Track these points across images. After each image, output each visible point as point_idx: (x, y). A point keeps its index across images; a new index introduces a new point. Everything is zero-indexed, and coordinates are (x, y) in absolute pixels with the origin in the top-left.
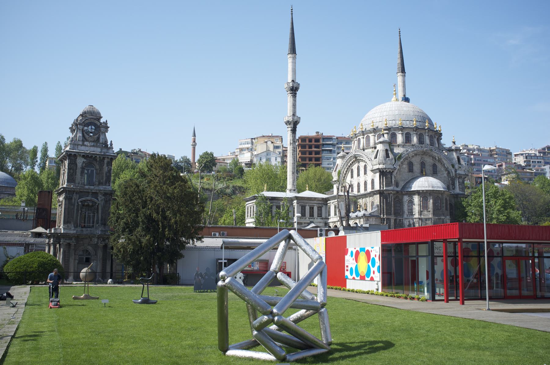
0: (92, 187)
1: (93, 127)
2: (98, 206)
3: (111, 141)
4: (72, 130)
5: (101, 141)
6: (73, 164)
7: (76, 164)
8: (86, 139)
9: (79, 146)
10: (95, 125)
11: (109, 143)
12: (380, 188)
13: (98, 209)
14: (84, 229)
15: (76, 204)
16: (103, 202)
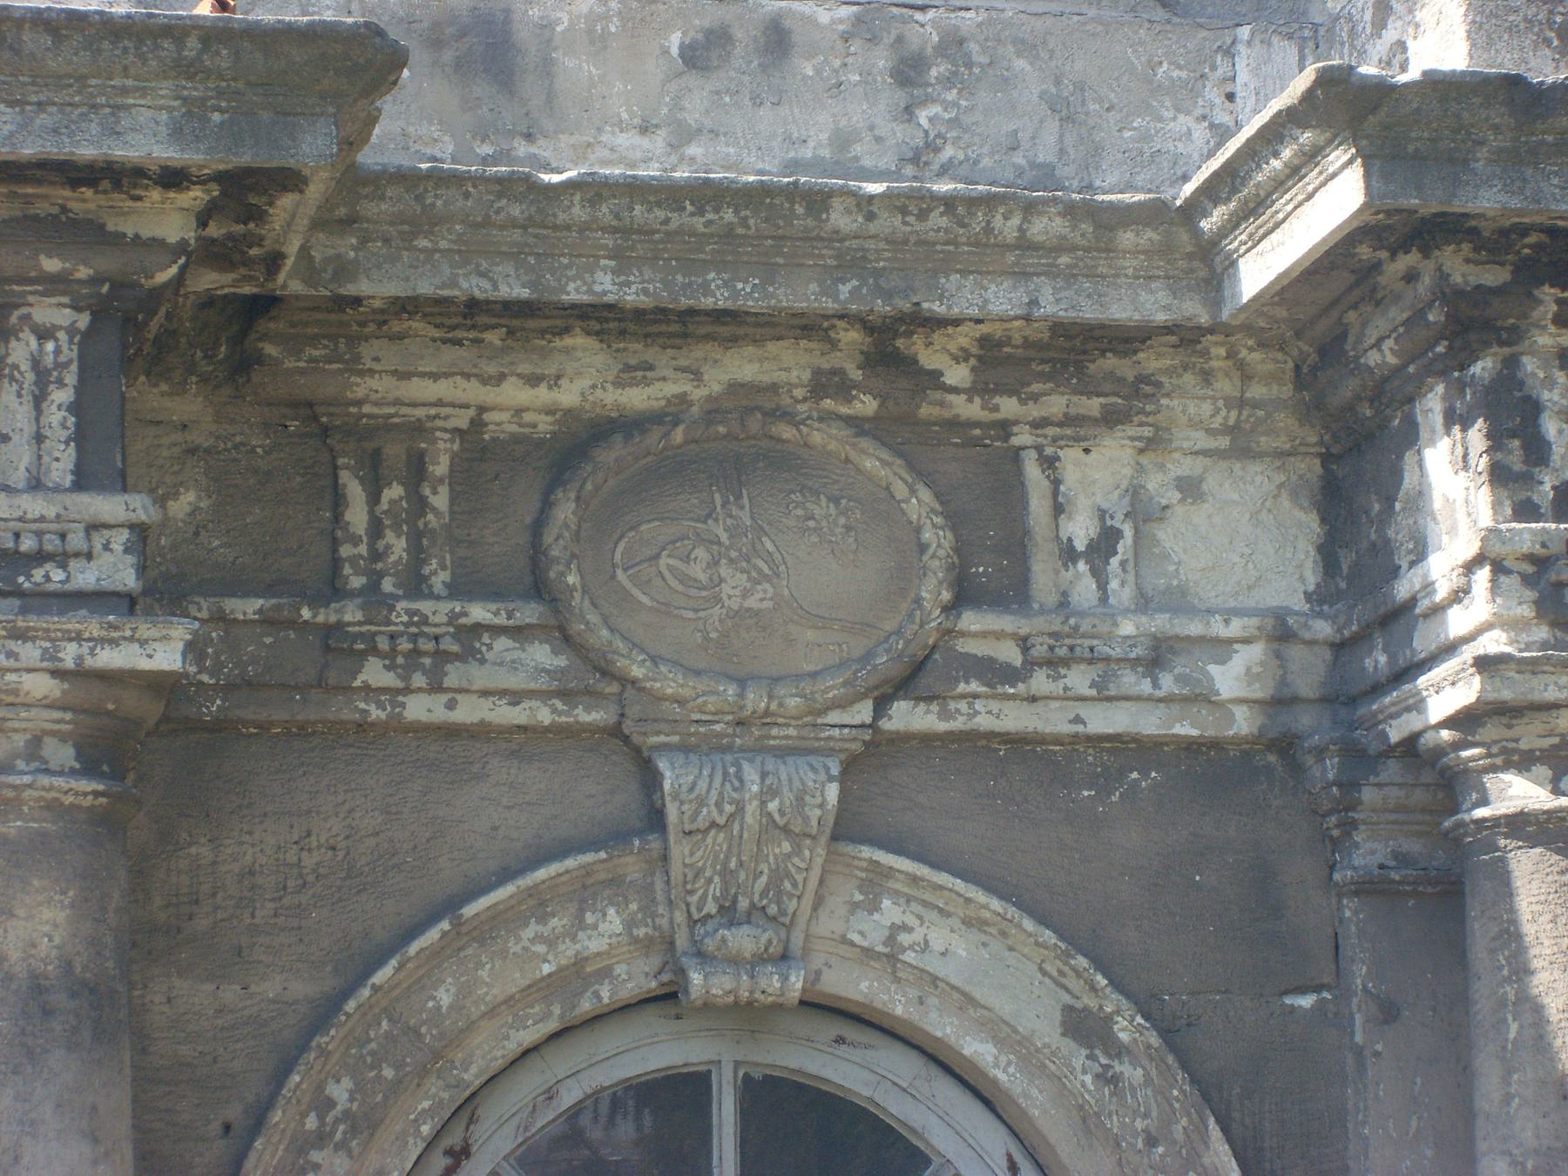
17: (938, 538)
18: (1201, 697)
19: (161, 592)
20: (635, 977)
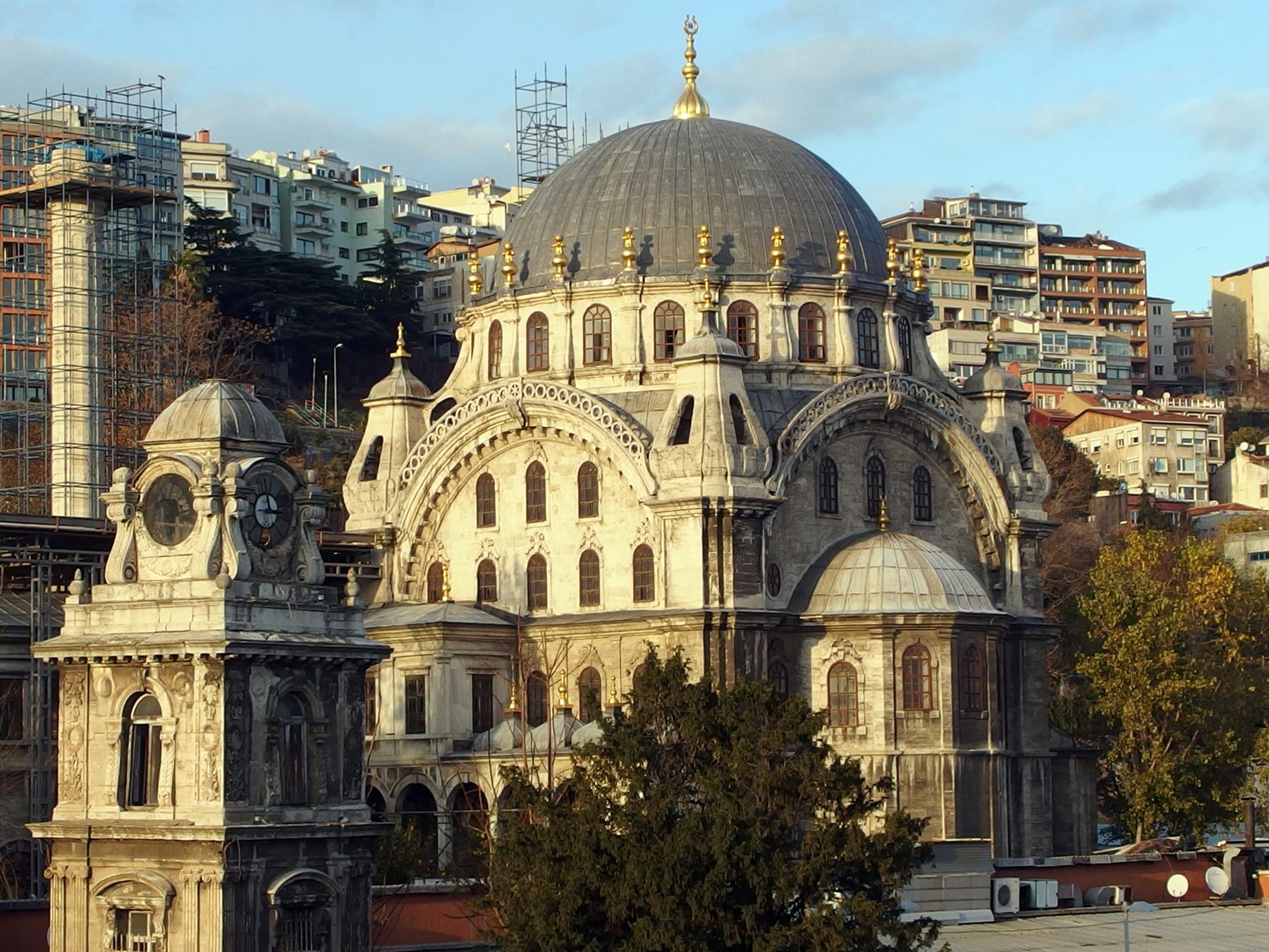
0: (307, 814)
9: (255, 611)
12: (706, 600)
16: (347, 880)
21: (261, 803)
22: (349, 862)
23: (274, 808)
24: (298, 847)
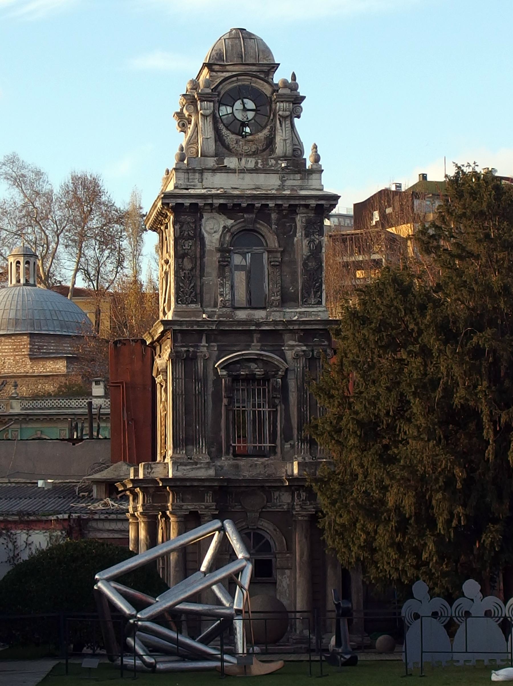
0: (260, 315)
1: (250, 104)
2: (284, 378)
3: (315, 147)
4: (183, 122)
5: (280, 148)
6: (190, 238)
7: (202, 239)
8: (227, 147)
9: (206, 175)
10: (257, 96)
11: (308, 155)
13: (285, 388)
14: (242, 462)
15: (211, 377)
16: (302, 362)
17: (265, 499)
18: (283, 508)
19: (216, 509)
20: (246, 527)
21: (215, 306)
22: (304, 348)
23: (224, 310)
24: (252, 337)
